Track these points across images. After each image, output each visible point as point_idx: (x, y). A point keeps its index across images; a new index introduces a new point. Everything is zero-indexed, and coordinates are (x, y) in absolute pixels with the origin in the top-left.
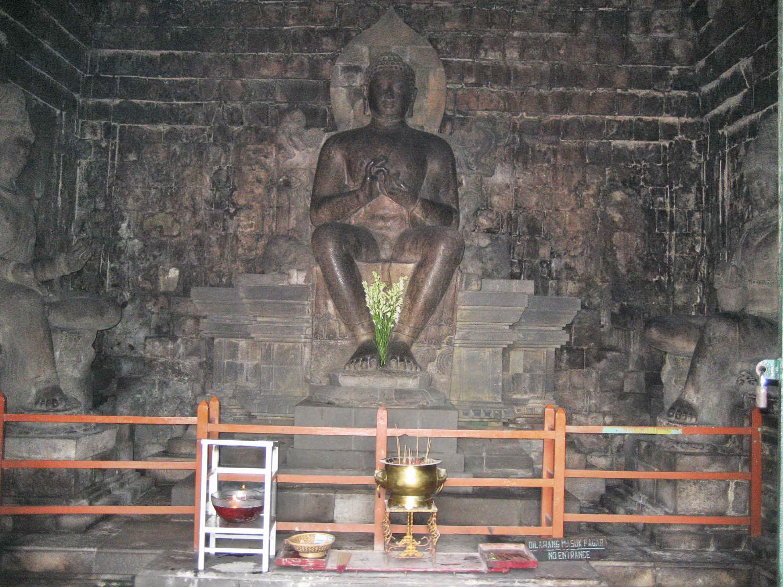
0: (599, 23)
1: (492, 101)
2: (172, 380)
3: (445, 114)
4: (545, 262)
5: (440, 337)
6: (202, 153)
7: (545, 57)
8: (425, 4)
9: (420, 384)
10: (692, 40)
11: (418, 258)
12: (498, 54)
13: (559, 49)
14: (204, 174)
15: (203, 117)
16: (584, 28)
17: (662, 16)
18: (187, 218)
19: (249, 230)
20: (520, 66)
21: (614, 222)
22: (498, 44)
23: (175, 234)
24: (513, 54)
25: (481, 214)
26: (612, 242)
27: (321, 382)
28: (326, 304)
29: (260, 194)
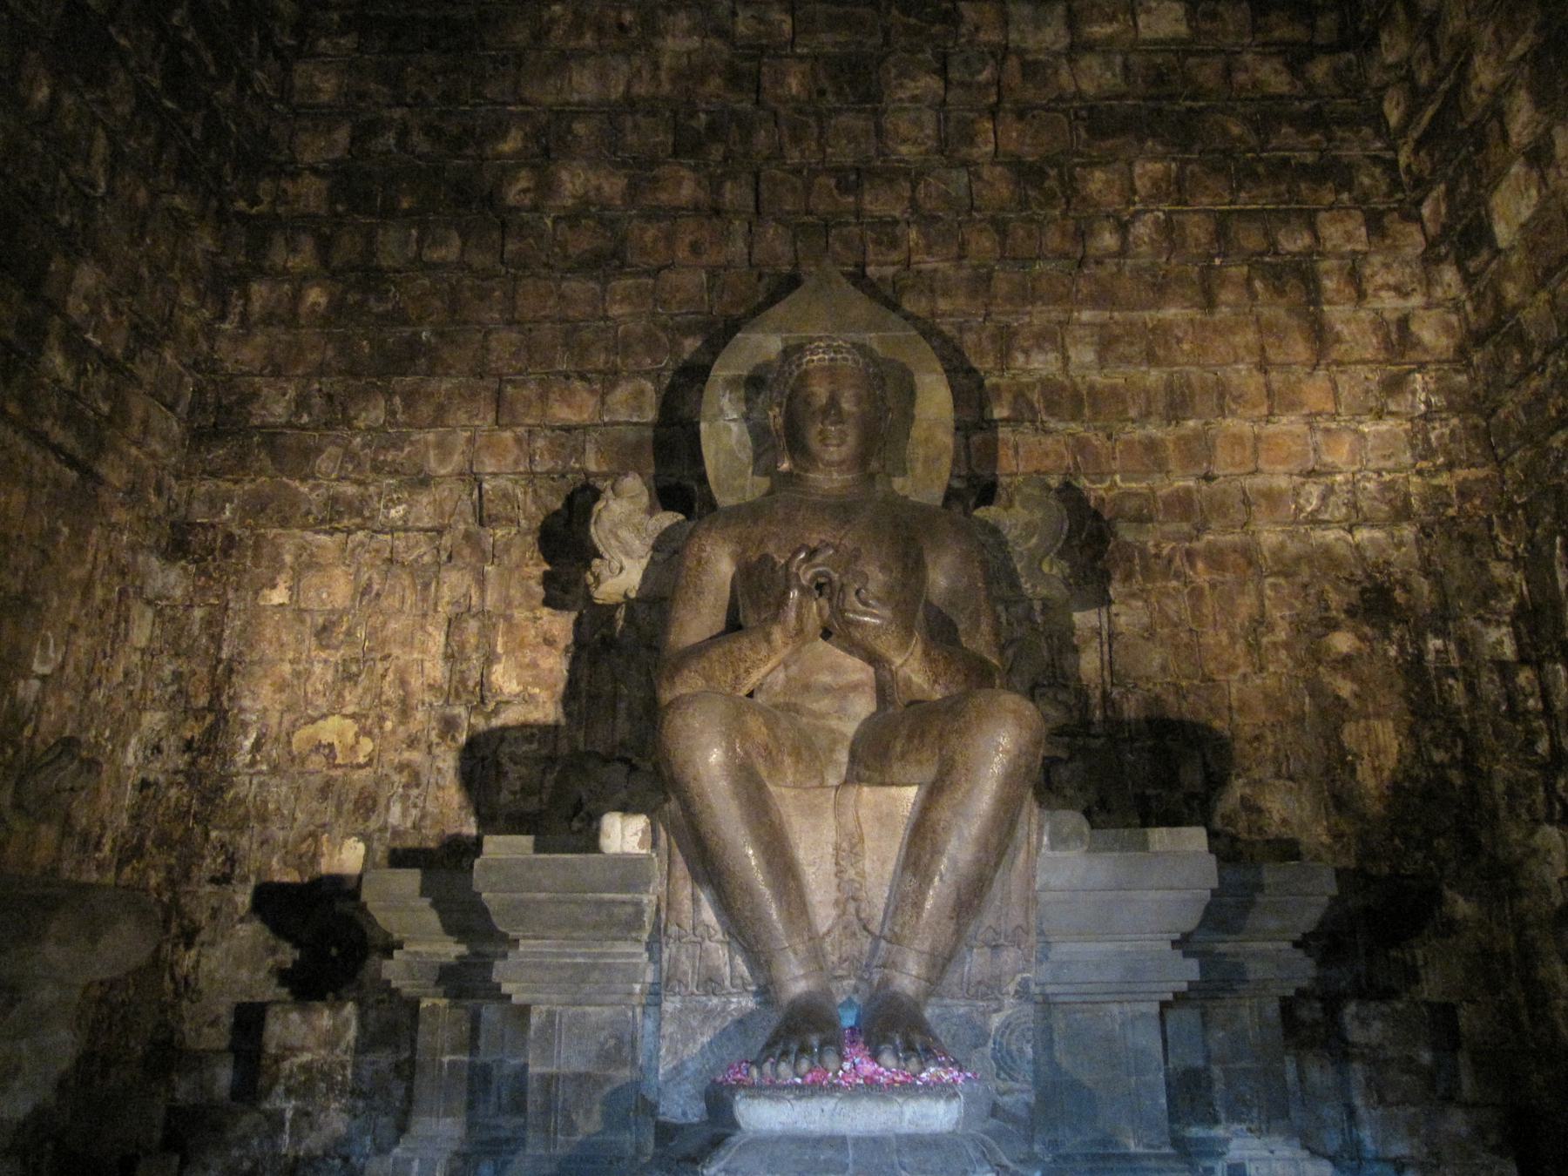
0: (1258, 285)
1: (1047, 454)
2: (325, 1109)
3: (949, 487)
4: (1194, 796)
5: (998, 978)
6: (426, 586)
7: (1151, 359)
8: (893, 264)
9: (967, 1118)
10: (1457, 307)
11: (930, 772)
12: (1052, 356)
13: (1179, 341)
14: (430, 629)
15: (430, 509)
16: (1227, 296)
17: (1387, 266)
18: (388, 725)
19: (525, 748)
20: (1096, 378)
21: (1338, 698)
22: (1051, 338)
23: (362, 760)
24: (1083, 355)
25: (1043, 695)
26: (1341, 746)
27: (684, 1114)
28: (695, 901)
29: (551, 670)
